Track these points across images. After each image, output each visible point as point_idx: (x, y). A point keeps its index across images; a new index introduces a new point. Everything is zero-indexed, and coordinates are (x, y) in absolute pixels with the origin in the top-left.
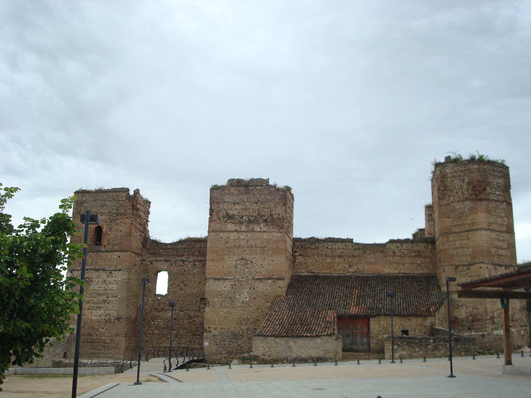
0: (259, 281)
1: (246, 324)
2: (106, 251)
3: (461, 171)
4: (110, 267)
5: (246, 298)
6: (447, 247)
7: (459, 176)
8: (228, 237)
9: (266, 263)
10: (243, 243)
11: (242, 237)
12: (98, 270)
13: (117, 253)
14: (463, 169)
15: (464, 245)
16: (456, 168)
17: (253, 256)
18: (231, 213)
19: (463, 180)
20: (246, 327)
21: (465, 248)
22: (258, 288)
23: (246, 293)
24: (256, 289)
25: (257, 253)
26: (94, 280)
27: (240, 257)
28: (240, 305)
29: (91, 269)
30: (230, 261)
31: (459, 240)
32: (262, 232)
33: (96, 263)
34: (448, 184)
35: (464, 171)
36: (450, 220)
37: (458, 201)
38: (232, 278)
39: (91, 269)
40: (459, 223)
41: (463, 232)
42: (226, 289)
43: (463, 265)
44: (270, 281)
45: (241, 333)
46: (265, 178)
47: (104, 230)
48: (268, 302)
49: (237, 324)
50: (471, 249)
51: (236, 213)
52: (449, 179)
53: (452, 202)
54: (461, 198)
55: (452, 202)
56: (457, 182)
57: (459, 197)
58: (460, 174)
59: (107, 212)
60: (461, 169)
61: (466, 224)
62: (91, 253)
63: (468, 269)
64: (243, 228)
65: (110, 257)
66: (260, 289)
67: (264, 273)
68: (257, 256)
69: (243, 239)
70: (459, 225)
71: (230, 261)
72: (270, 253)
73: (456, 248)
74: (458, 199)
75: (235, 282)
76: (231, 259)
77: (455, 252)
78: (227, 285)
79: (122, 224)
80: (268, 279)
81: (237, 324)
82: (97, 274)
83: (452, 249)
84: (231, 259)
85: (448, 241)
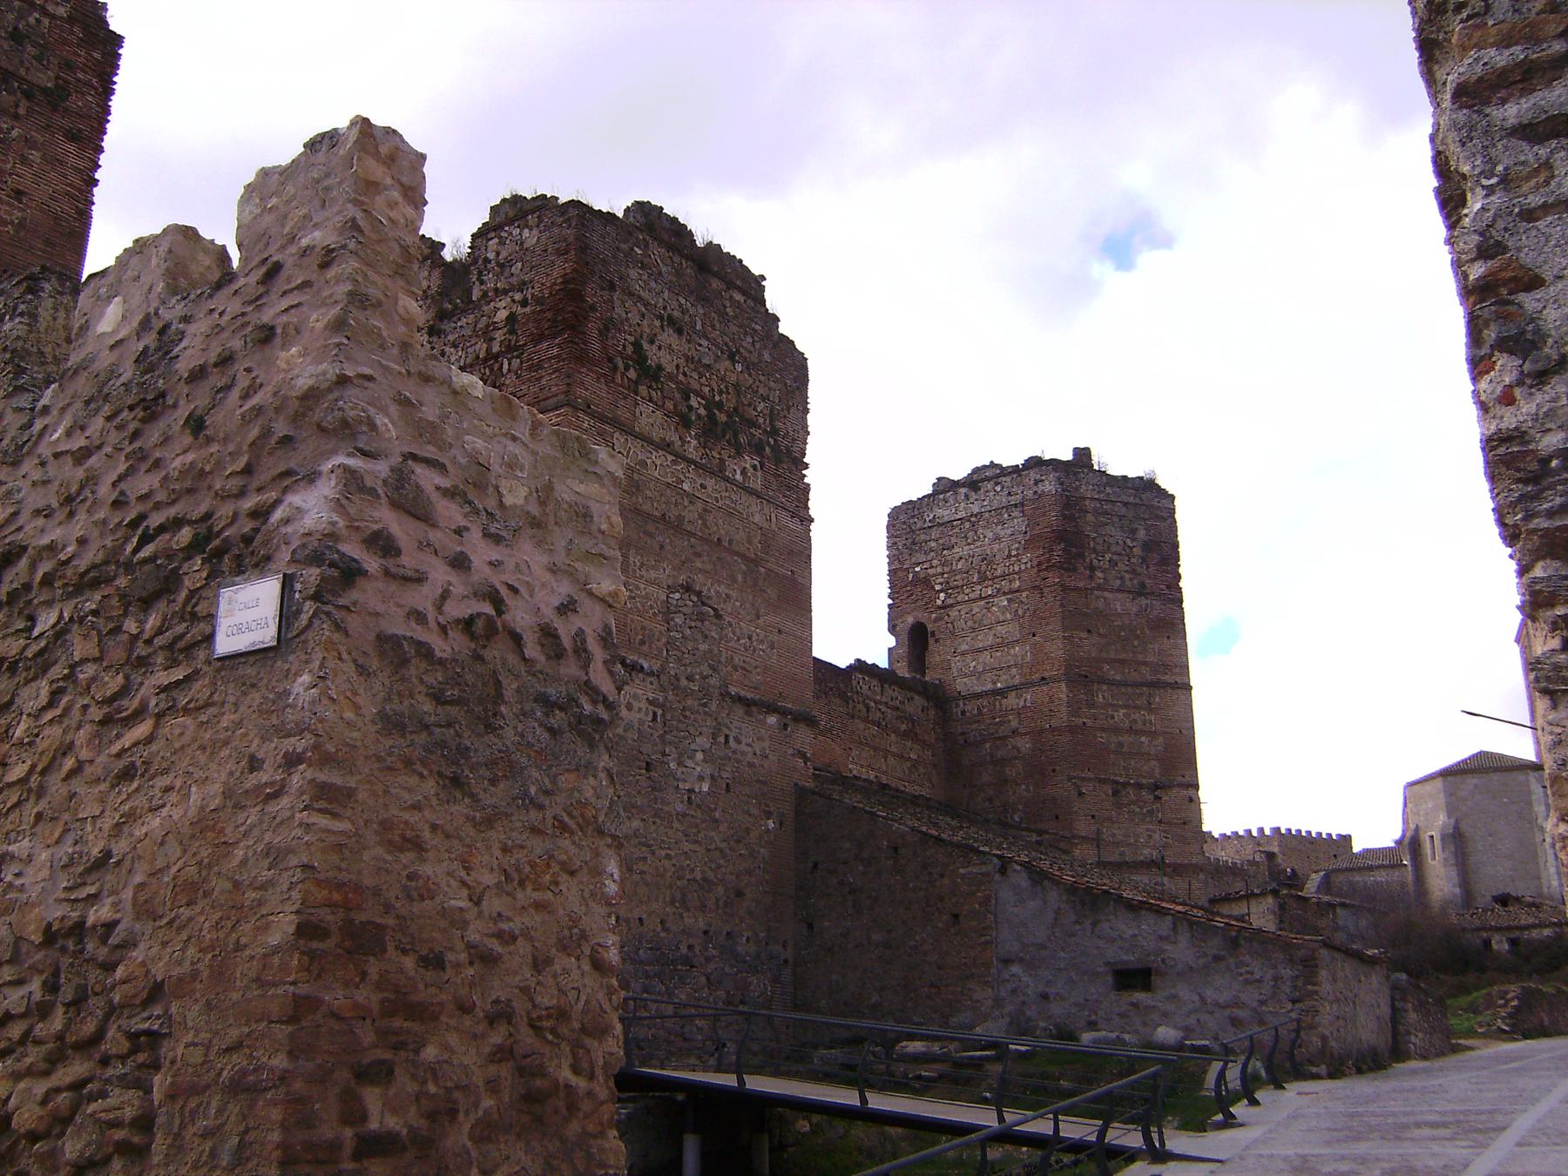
0: (739, 711)
1: (703, 907)
3: (1126, 504)
5: (701, 778)
6: (1089, 723)
7: (1121, 517)
8: (644, 464)
9: (762, 634)
10: (691, 513)
11: (686, 486)
14: (1131, 500)
15: (1139, 726)
16: (1108, 490)
17: (722, 589)
18: (654, 355)
19: (1134, 531)
20: (701, 924)
21: (1142, 733)
22: (738, 741)
23: (699, 756)
24: (732, 743)
25: (734, 580)
27: (682, 579)
28: (680, 807)
30: (651, 582)
31: (1126, 707)
32: (746, 489)
34: (1088, 530)
35: (1135, 505)
36: (1095, 639)
37: (1119, 590)
38: (656, 667)
40: (1123, 656)
41: (1135, 685)
42: (634, 717)
43: (1139, 786)
44: (772, 720)
45: (684, 950)
46: (756, 271)
48: (769, 815)
49: (673, 902)
50: (1161, 739)
51: (668, 362)
52: (1090, 517)
53: (1100, 588)
54: (1128, 583)
55: (1100, 588)
56: (1115, 533)
57: (1122, 578)
58: (1123, 511)
60: (1124, 498)
61: (1145, 663)
63: (1158, 798)
64: (692, 448)
66: (743, 747)
67: (756, 678)
68: (734, 594)
69: (692, 498)
70: (1123, 662)
71: (651, 582)
72: (772, 592)
73: (1116, 730)
74: (1118, 582)
75: (663, 689)
76: (653, 574)
77: (1114, 739)
78: (636, 697)
79: (35, 156)
80: (772, 709)
81: (673, 902)
83: (1103, 730)
84: (653, 574)
85: (1091, 705)
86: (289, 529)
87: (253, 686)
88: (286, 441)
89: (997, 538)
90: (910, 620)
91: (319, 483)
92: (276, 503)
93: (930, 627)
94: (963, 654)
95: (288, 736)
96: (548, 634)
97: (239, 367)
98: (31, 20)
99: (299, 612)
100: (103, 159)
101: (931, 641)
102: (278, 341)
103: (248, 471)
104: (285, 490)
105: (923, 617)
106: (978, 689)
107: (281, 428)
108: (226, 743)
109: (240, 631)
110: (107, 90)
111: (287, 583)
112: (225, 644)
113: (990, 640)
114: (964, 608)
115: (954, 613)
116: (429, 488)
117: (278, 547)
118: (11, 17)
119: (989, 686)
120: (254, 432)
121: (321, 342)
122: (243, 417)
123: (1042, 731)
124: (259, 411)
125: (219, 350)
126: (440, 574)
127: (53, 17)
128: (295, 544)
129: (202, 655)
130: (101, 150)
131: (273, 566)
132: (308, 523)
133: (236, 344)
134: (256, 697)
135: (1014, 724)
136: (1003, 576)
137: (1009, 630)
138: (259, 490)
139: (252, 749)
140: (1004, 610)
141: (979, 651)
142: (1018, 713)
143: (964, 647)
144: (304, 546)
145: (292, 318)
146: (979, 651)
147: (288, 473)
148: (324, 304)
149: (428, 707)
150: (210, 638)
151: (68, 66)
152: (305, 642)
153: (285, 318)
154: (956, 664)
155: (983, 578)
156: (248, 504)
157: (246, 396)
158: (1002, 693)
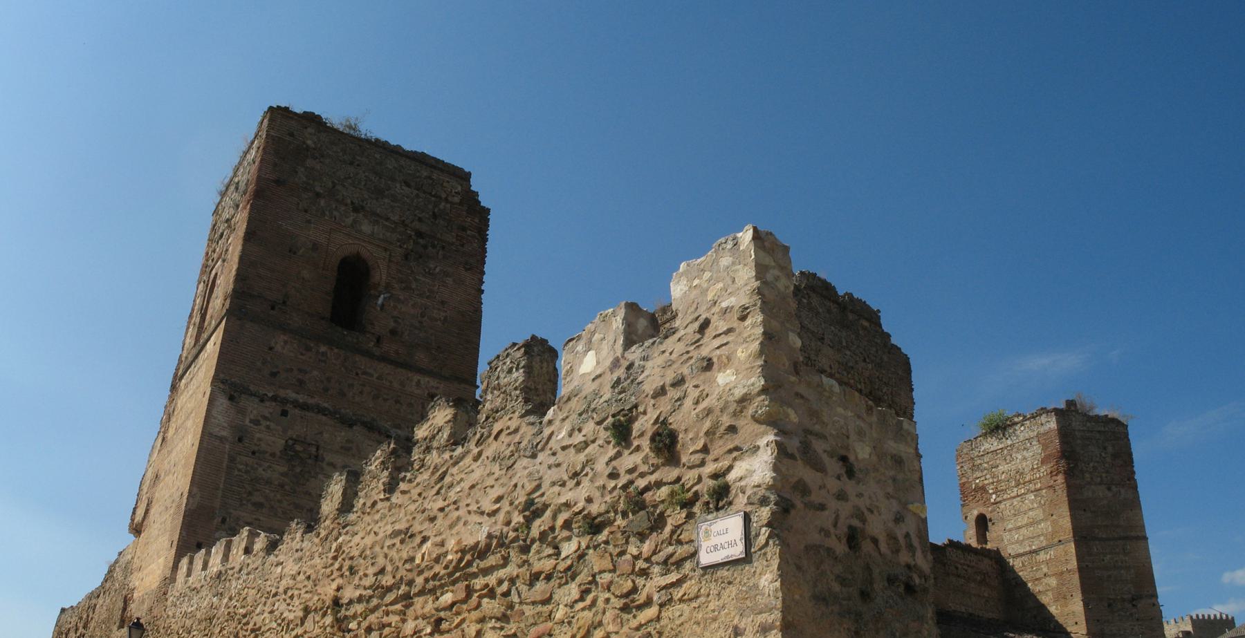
2: (384, 359)
4: (398, 427)
6: (1090, 565)
12: (349, 423)
13: (425, 380)
26: (329, 457)
29: (321, 411)
33: (342, 394)
39: (321, 411)
43: (1123, 600)
47: (380, 275)
59: (396, 218)
62: (323, 349)
65: (396, 385)
79: (449, 281)
82: (342, 435)
86: (743, 483)
87: (730, 583)
88: (732, 429)
89: (1025, 458)
90: (976, 513)
91: (759, 453)
92: (730, 468)
93: (988, 516)
94: (1010, 530)
95: (760, 613)
96: (892, 537)
97: (689, 385)
98: (442, 206)
99: (757, 535)
100: (485, 278)
101: (990, 524)
102: (715, 366)
103: (705, 450)
104: (735, 459)
105: (983, 510)
106: (1021, 551)
107: (726, 421)
108: (715, 619)
109: (716, 548)
110: (484, 239)
111: (747, 519)
112: (706, 558)
113: (1025, 521)
114: (1008, 503)
115: (1002, 506)
116: (820, 451)
117: (736, 495)
118: (430, 207)
119: (1028, 549)
120: (707, 424)
121: (748, 365)
122: (697, 416)
123: (1062, 573)
124: (709, 412)
125: (674, 375)
126: (833, 504)
127: (452, 203)
128: (749, 492)
129: (688, 565)
130: (484, 273)
131: (734, 507)
132: (756, 479)
133: (686, 370)
134: (733, 590)
135: (1045, 570)
136: (1030, 482)
137: (1038, 514)
138: (716, 460)
139: (736, 621)
140: (1032, 502)
141: (1020, 528)
142: (1047, 562)
143: (1010, 526)
144: (755, 493)
145: (724, 350)
146: (1020, 528)
147: (737, 449)
148: (745, 341)
149: (837, 588)
150: (694, 554)
151: (464, 229)
152: (765, 554)
153: (718, 352)
154: (1006, 536)
155: (1017, 486)
156: (710, 468)
157: (697, 403)
158: (1036, 552)
